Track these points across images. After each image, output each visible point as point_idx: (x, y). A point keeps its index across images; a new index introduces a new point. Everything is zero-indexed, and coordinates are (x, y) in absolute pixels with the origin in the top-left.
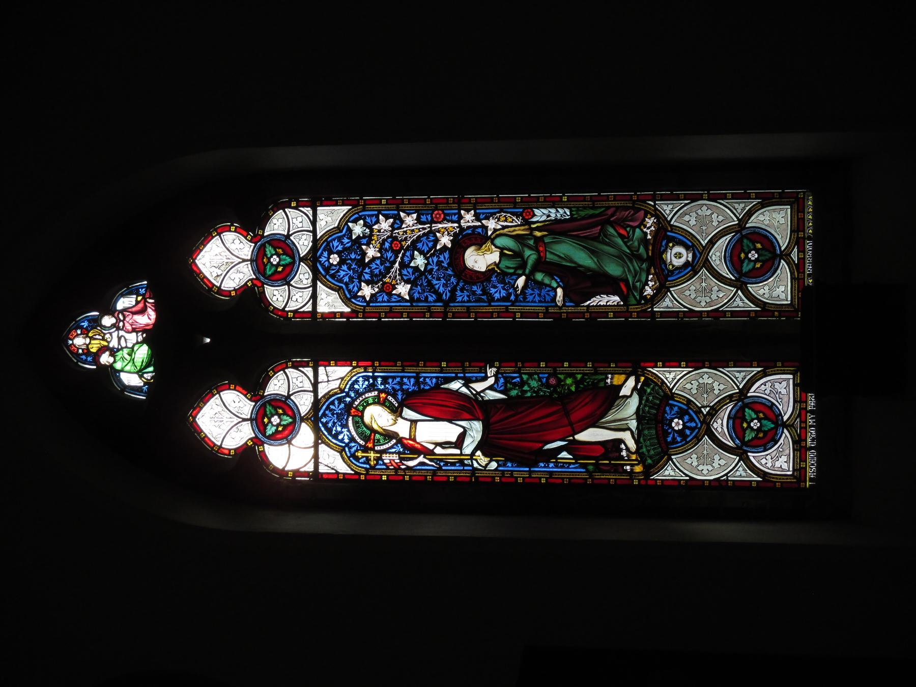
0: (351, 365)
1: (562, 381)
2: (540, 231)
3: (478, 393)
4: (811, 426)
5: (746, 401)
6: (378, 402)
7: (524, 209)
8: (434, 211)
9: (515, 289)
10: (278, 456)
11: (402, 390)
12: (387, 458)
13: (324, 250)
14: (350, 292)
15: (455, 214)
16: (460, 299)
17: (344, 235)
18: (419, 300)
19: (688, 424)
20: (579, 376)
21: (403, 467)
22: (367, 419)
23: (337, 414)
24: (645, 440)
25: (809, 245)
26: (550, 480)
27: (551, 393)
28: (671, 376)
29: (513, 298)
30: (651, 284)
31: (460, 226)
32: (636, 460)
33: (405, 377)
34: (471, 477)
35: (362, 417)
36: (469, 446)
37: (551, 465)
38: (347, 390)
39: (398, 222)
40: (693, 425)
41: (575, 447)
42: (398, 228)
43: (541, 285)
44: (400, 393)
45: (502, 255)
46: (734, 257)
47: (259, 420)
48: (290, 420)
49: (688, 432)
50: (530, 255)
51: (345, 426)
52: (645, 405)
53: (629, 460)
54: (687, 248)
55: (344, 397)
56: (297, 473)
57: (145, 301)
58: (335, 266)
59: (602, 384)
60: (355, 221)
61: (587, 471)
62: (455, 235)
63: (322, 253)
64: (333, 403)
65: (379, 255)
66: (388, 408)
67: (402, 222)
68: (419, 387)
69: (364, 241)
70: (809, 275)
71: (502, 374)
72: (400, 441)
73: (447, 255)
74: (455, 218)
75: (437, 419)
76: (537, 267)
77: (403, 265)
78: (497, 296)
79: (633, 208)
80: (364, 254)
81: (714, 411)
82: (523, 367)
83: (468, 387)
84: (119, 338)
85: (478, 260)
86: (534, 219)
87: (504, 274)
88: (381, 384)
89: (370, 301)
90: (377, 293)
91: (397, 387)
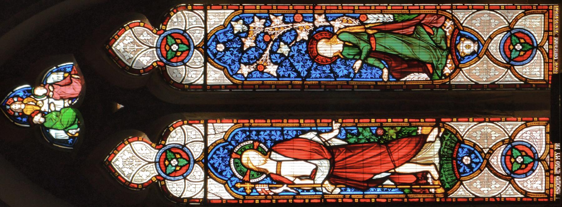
0: (233, 123)
1: (387, 132)
2: (372, 29)
3: (327, 141)
4: (557, 160)
5: (513, 144)
6: (252, 148)
7: (361, 14)
8: (295, 14)
9: (354, 70)
10: (175, 188)
11: (271, 140)
12: (259, 188)
13: (213, 41)
14: (232, 70)
15: (310, 17)
16: (313, 76)
17: (228, 31)
18: (283, 76)
19: (474, 160)
20: (399, 128)
21: (271, 194)
22: (244, 160)
23: (222, 157)
24: (444, 171)
25: (556, 41)
26: (378, 200)
27: (379, 140)
28: (463, 127)
29: (352, 75)
30: (449, 65)
31: (314, 25)
32: (438, 185)
33: (273, 130)
34: (321, 199)
35: (240, 159)
36: (320, 177)
37: (379, 190)
38: (229, 140)
39: (268, 21)
40: (477, 160)
41: (393, 176)
42: (269, 26)
43: (372, 66)
44: (269, 142)
45: (345, 46)
46: (506, 49)
47: (162, 163)
48: (186, 162)
49: (474, 165)
50: (365, 47)
51: (229, 165)
52: (445, 148)
53: (434, 185)
54: (474, 41)
55: (227, 145)
56: (190, 199)
57: (71, 77)
58: (221, 52)
59: (414, 134)
60: (237, 21)
61: (404, 193)
62: (311, 32)
63: (211, 43)
64: (218, 149)
65: (254, 45)
66: (261, 152)
67: (271, 22)
68: (284, 138)
69: (244, 35)
70: (556, 60)
71: (344, 127)
72: (269, 175)
73: (304, 45)
74: (311, 20)
75: (296, 159)
76: (369, 55)
77: (272, 52)
78: (340, 74)
79: (437, 14)
80: (243, 44)
81: (491, 151)
82: (359, 122)
83: (319, 137)
84: (49, 105)
85: (327, 49)
86: (368, 22)
87: (346, 59)
88: (256, 135)
89: (247, 77)
90: (253, 71)
91: (267, 138)
